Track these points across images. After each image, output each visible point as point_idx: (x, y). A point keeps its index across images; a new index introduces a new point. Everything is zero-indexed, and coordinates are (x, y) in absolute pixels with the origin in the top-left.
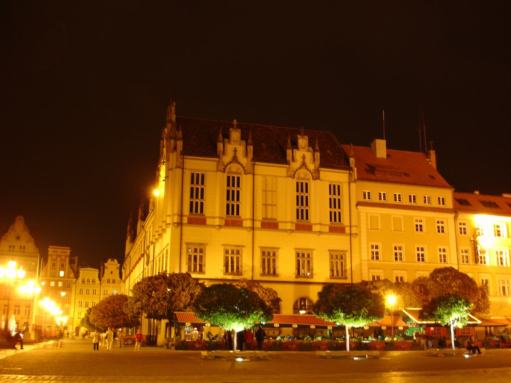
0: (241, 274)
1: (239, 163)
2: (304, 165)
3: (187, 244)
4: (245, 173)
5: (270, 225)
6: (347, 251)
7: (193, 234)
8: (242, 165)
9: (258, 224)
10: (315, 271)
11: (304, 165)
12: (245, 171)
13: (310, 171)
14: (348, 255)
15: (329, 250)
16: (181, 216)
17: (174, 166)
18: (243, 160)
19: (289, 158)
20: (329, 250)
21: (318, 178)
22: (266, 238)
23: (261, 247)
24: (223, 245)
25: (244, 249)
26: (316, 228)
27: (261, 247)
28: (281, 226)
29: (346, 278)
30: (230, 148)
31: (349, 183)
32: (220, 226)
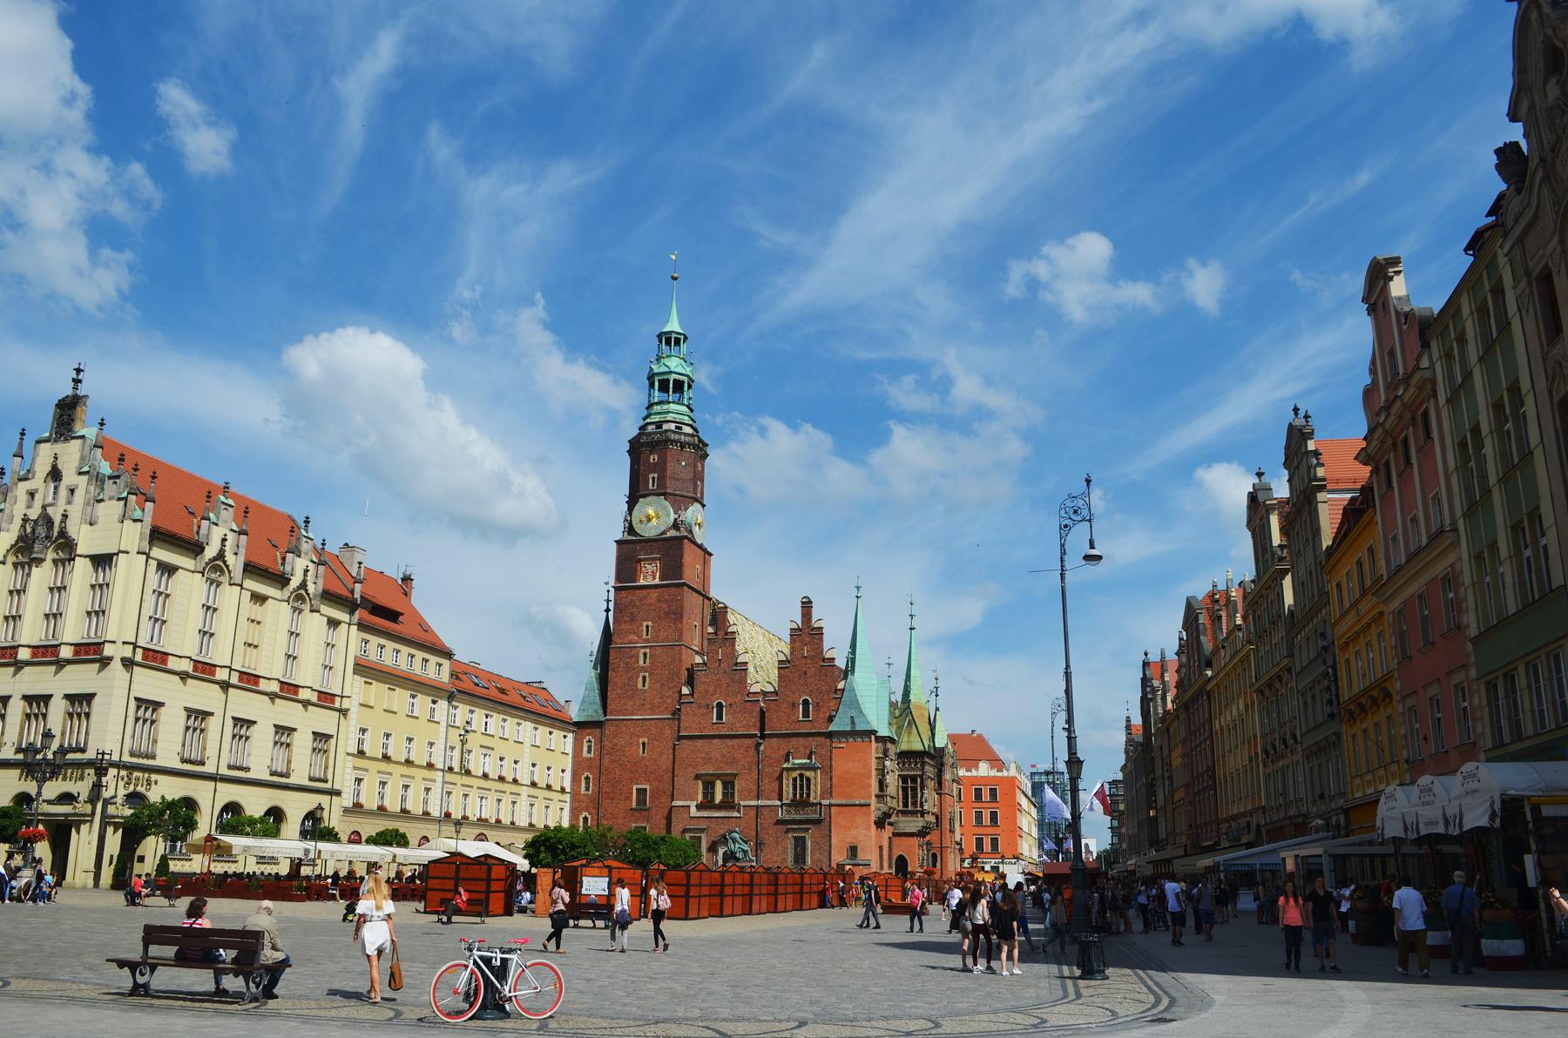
0: (202, 763)
2: (303, 585)
5: (250, 680)
7: (148, 683)
9: (234, 679)
10: (293, 766)
11: (303, 585)
14: (333, 741)
16: (135, 646)
18: (230, 558)
19: (288, 568)
22: (243, 704)
24: (186, 709)
26: (304, 694)
28: (264, 685)
30: (217, 534)
32: (184, 676)
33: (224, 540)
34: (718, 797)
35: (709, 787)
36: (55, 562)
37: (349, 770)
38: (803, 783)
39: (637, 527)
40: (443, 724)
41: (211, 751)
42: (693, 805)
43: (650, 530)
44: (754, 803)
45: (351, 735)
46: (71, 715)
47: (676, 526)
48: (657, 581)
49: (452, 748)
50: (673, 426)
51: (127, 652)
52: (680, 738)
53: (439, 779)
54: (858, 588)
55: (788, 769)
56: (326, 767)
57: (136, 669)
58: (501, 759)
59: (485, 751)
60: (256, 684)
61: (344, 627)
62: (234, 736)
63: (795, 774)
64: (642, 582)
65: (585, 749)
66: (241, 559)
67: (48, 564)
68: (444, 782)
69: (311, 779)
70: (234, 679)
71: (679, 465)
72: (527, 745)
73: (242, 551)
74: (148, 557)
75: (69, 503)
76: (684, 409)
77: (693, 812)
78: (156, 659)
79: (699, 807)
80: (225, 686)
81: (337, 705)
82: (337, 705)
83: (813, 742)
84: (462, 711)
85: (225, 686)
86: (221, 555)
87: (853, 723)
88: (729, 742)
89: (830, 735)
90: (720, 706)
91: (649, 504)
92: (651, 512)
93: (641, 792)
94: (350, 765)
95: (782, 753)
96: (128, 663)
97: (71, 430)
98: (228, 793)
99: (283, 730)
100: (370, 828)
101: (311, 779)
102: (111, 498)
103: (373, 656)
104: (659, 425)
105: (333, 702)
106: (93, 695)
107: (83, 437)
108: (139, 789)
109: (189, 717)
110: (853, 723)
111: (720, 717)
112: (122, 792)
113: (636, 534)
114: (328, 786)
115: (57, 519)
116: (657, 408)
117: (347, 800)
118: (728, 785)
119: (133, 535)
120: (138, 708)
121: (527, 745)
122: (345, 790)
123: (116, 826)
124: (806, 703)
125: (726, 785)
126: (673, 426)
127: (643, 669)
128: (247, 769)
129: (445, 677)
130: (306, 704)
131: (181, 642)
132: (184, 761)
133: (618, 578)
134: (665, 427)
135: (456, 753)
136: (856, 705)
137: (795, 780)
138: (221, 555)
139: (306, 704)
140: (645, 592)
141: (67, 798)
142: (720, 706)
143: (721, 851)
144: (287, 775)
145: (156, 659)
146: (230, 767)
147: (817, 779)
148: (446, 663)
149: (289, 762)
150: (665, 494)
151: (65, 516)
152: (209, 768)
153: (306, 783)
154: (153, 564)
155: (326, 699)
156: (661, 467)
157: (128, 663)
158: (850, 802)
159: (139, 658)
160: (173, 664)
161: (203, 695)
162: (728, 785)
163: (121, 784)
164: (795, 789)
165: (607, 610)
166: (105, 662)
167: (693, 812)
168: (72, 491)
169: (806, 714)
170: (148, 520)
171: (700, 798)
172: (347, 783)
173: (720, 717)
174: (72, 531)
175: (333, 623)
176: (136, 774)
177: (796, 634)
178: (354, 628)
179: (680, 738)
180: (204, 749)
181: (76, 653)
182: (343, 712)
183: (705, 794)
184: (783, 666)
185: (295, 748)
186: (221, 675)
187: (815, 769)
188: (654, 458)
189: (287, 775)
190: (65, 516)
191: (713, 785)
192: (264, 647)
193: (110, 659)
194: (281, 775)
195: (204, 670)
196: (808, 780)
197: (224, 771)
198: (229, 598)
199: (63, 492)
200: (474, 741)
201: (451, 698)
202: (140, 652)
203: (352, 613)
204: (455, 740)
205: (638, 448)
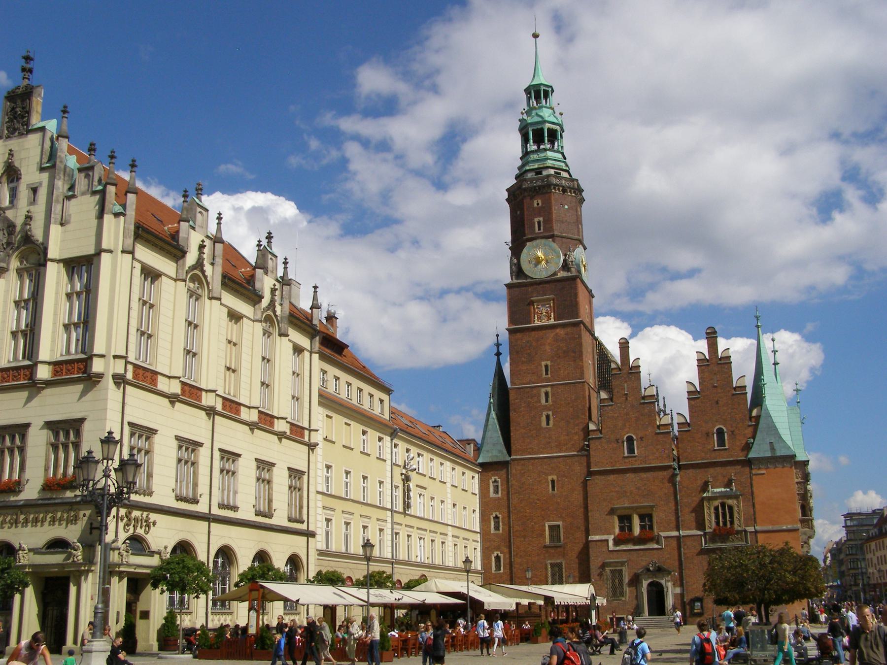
1: (203, 272)
3: (130, 424)
4: (210, 298)
6: (303, 473)
8: (206, 277)
10: (274, 506)
12: (209, 291)
13: (276, 316)
14: (305, 477)
15: (289, 469)
17: (120, 249)
18: (208, 268)
20: (289, 469)
21: (283, 334)
22: (231, 435)
23: (221, 450)
24: (178, 438)
25: (200, 448)
26: (281, 426)
27: (221, 450)
29: (302, 522)
31: (311, 353)
33: (202, 247)
34: (637, 531)
35: (625, 520)
36: (19, 272)
37: (320, 510)
38: (725, 511)
39: (526, 267)
40: (389, 462)
41: (203, 488)
42: (611, 539)
43: (541, 272)
44: (675, 533)
45: (319, 473)
46: (55, 447)
47: (566, 266)
48: (552, 321)
49: (397, 487)
50: (552, 172)
51: (118, 367)
52: (590, 473)
53: (389, 520)
54: (757, 318)
55: (710, 499)
56: (301, 507)
57: (128, 388)
58: (432, 498)
59: (420, 490)
60: (238, 412)
61: (307, 354)
62: (222, 471)
63: (717, 503)
64: (537, 323)
65: (492, 489)
66: (219, 270)
67: (12, 275)
68: (393, 523)
69: (290, 520)
70: (219, 408)
71: (561, 206)
72: (449, 485)
73: (219, 261)
74: (134, 258)
75: (33, 202)
76: (560, 156)
77: (611, 543)
78: (145, 378)
79: (617, 542)
80: (211, 412)
81: (306, 439)
82: (306, 439)
83: (732, 471)
84: (402, 451)
85: (211, 412)
86: (199, 265)
87: (773, 449)
88: (644, 475)
89: (749, 463)
90: (630, 440)
91: (537, 247)
92: (540, 254)
93: (554, 529)
94: (320, 504)
95: (700, 482)
96: (120, 380)
97: (27, 124)
98: (223, 535)
99: (264, 465)
100: (359, 571)
101: (290, 520)
102: (83, 194)
103: (331, 389)
104: (538, 171)
105: (303, 436)
106: (82, 420)
107: (43, 129)
108: (140, 531)
109: (180, 447)
110: (773, 449)
111: (631, 450)
112: (123, 536)
113: (527, 277)
114: (304, 527)
115: (19, 221)
116: (534, 157)
117: (319, 543)
118: (646, 518)
119: (116, 231)
120: (132, 435)
121: (449, 485)
122: (318, 531)
123: (121, 575)
124: (720, 432)
125: (642, 518)
126: (552, 172)
127: (546, 408)
128: (235, 508)
129: (387, 416)
130: (281, 436)
131: (167, 359)
132: (179, 498)
133: (512, 319)
134: (545, 173)
135: (399, 493)
136: (773, 429)
137: (716, 509)
138: (199, 265)
139: (281, 436)
140: (541, 333)
141: (58, 545)
142: (630, 440)
143: (645, 584)
144: (270, 516)
145: (145, 378)
146: (221, 506)
147: (739, 507)
148: (385, 397)
149: (270, 501)
150: (552, 237)
151: (29, 218)
152: (202, 507)
153: (286, 523)
154: (138, 266)
155: (298, 433)
156: (546, 211)
157: (120, 380)
158: (776, 527)
159: (130, 376)
160: (163, 384)
161: (194, 423)
162: (646, 518)
163: (121, 525)
164: (717, 517)
165: (498, 354)
166: (91, 380)
167: (611, 543)
168: (35, 190)
169: (721, 442)
170: (131, 212)
171: (617, 531)
172: (319, 524)
173: (631, 450)
174: (38, 234)
175: (298, 350)
176: (136, 513)
177: (703, 364)
178: (316, 357)
179: (590, 473)
180: (195, 485)
181: (55, 373)
182: (312, 447)
183: (622, 529)
184: (693, 396)
185: (275, 486)
186: (208, 400)
187: (736, 497)
188: (537, 202)
189: (270, 516)
190: (29, 218)
191: (629, 518)
192: (244, 372)
193: (100, 376)
194: (265, 516)
195: (190, 394)
196: (731, 508)
197: (216, 511)
198: (213, 314)
199: (24, 193)
200: (415, 479)
201: (393, 434)
202: (130, 368)
203: (312, 338)
204: (398, 481)
205: (518, 197)
